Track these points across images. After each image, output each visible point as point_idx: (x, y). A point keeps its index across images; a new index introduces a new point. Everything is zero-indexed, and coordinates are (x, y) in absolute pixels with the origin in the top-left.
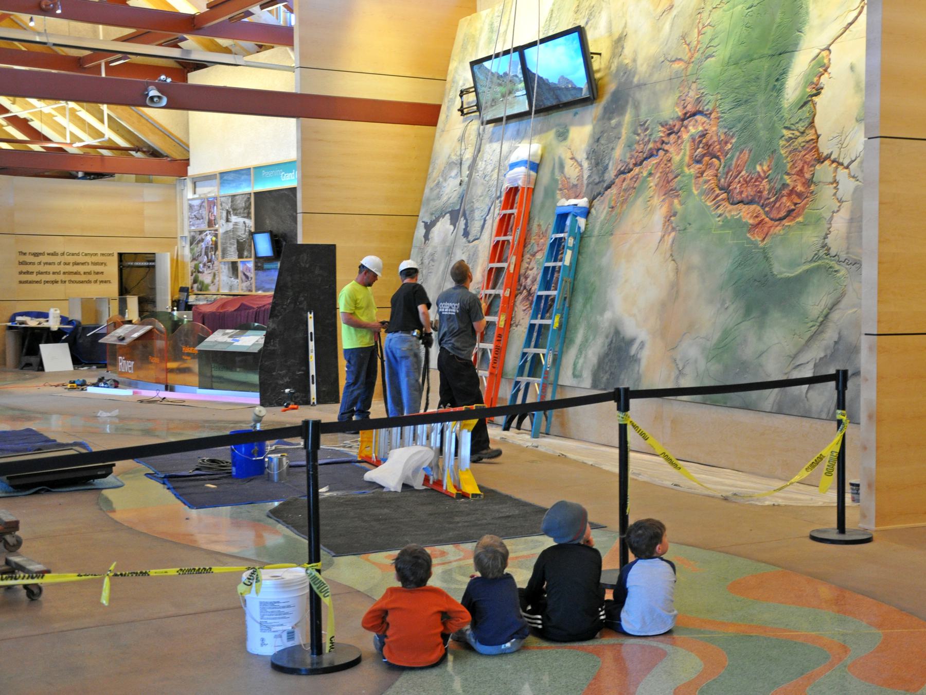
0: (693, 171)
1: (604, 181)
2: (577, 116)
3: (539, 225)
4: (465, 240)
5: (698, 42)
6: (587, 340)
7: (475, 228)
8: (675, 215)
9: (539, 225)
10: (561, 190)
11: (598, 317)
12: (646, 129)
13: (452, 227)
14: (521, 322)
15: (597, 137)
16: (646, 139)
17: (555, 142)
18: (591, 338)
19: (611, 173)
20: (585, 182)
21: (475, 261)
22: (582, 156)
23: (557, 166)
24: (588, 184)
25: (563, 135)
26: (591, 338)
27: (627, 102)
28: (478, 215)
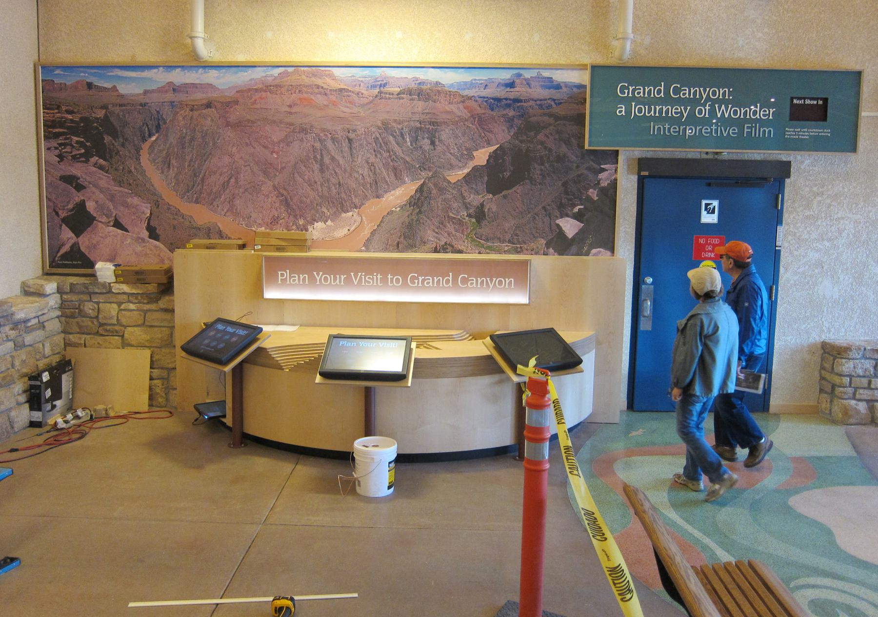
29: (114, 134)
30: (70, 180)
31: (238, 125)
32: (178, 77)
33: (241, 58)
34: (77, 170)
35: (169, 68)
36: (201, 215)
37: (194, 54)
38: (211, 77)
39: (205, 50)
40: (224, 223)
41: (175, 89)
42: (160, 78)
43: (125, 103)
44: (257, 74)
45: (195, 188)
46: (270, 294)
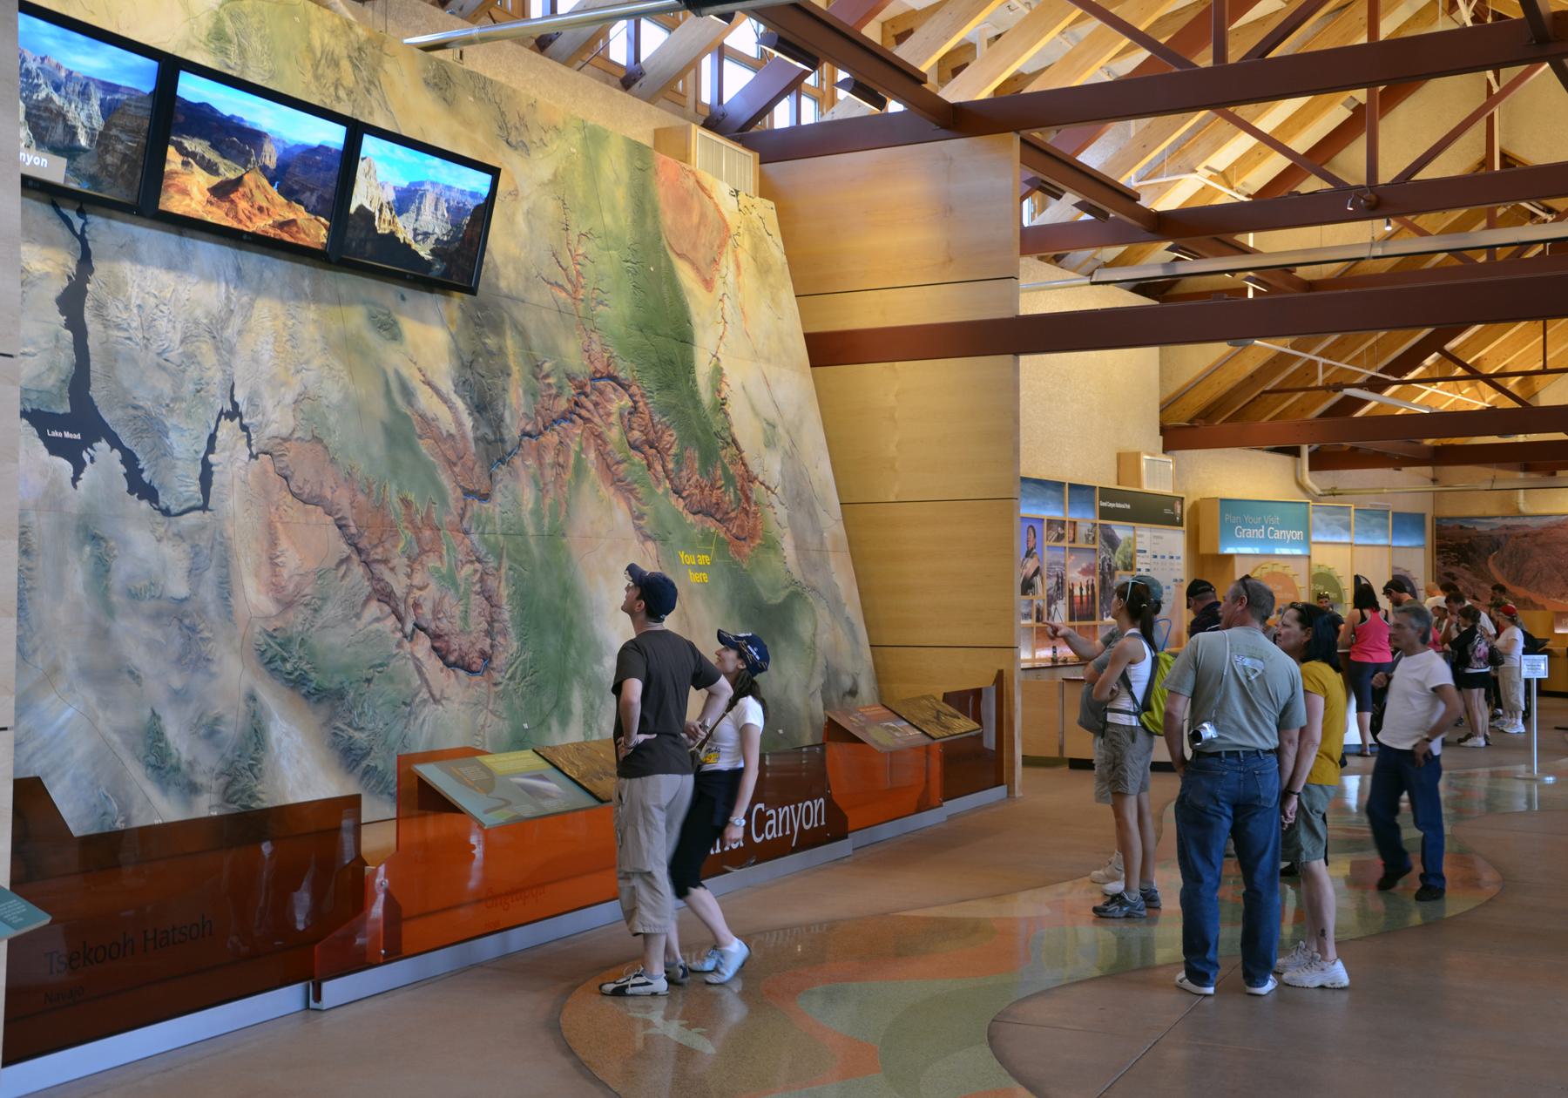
0: (637, 458)
1: (502, 441)
2: (406, 306)
3: (406, 503)
4: (145, 504)
5: (579, 274)
6: (592, 707)
7: (182, 484)
8: (640, 517)
9: (406, 503)
10: (420, 437)
11: (596, 667)
12: (547, 376)
13: (66, 466)
14: (448, 692)
15: (467, 358)
16: (554, 391)
17: (372, 338)
18: (598, 702)
19: (513, 428)
20: (470, 435)
21: (225, 563)
22: (447, 386)
23: (394, 386)
24: (477, 440)
25: (388, 328)
26: (598, 702)
27: (503, 322)
28: (184, 444)
29: (1474, 551)
30: (1449, 575)
31: (1542, 545)
32: (1509, 522)
33: (1544, 511)
34: (1454, 570)
35: (1504, 517)
36: (1521, 592)
37: (1519, 511)
38: (1528, 521)
39: (1523, 507)
40: (1535, 597)
41: (1507, 528)
42: (1500, 522)
43: (1480, 535)
44: (1553, 519)
45: (1518, 580)
46: (1558, 631)
